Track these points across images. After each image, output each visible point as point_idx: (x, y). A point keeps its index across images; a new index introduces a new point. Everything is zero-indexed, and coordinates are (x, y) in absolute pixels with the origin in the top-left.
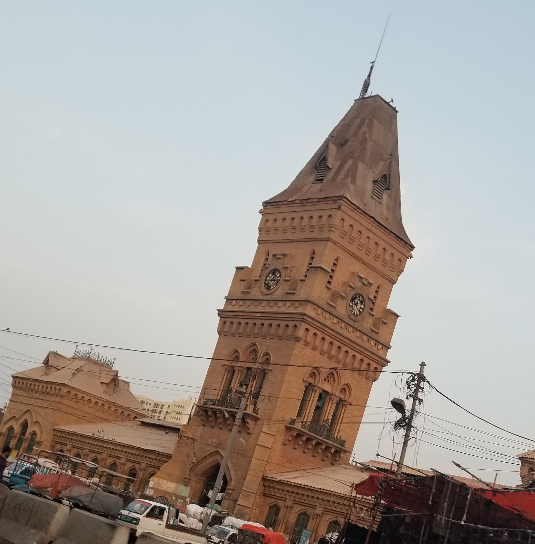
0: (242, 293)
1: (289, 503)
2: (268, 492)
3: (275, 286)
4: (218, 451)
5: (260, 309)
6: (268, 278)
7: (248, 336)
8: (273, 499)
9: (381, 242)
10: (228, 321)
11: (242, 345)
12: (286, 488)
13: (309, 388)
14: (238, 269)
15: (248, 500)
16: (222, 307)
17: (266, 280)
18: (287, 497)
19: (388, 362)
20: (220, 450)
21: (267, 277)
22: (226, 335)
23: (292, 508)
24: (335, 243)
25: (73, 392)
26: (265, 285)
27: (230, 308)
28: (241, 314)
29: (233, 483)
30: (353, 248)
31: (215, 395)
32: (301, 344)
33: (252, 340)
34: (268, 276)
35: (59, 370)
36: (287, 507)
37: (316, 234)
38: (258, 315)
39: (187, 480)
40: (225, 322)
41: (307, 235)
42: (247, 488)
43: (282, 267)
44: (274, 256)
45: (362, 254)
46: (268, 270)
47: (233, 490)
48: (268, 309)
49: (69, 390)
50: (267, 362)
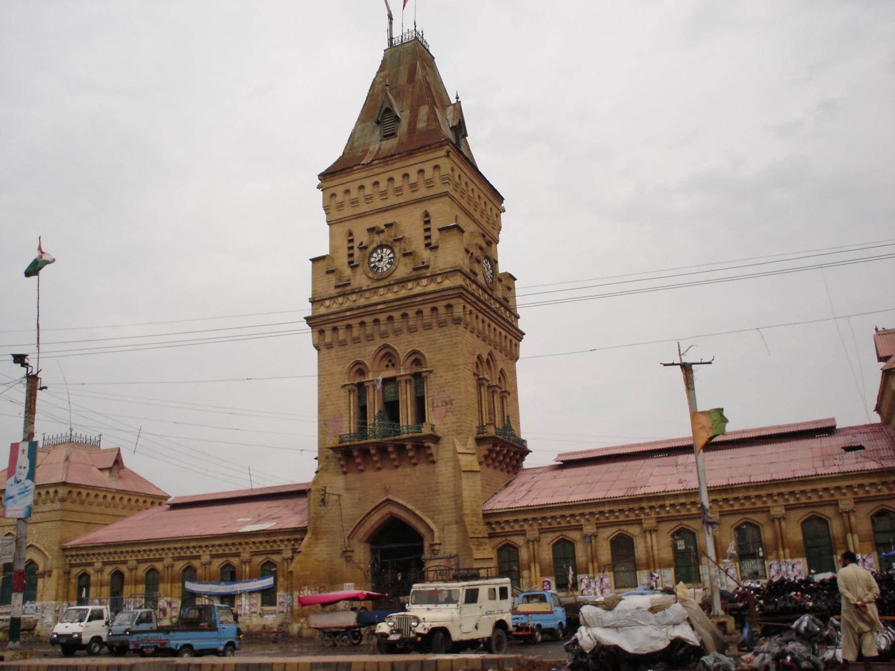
0: (337, 287)
1: (533, 533)
3: (389, 266)
4: (388, 500)
5: (376, 299)
6: (373, 260)
7: (370, 338)
9: (482, 196)
11: (368, 353)
13: (480, 382)
14: (314, 260)
16: (309, 313)
18: (526, 527)
19: (523, 334)
20: (390, 497)
21: (369, 259)
22: (329, 346)
24: (452, 198)
25: (76, 490)
27: (322, 310)
28: (348, 313)
29: (436, 534)
30: (464, 203)
31: (347, 426)
33: (379, 342)
36: (533, 541)
37: (423, 192)
38: (380, 307)
41: (408, 196)
42: (474, 533)
43: (391, 240)
44: (371, 230)
45: (471, 210)
48: (391, 296)
50: (418, 362)
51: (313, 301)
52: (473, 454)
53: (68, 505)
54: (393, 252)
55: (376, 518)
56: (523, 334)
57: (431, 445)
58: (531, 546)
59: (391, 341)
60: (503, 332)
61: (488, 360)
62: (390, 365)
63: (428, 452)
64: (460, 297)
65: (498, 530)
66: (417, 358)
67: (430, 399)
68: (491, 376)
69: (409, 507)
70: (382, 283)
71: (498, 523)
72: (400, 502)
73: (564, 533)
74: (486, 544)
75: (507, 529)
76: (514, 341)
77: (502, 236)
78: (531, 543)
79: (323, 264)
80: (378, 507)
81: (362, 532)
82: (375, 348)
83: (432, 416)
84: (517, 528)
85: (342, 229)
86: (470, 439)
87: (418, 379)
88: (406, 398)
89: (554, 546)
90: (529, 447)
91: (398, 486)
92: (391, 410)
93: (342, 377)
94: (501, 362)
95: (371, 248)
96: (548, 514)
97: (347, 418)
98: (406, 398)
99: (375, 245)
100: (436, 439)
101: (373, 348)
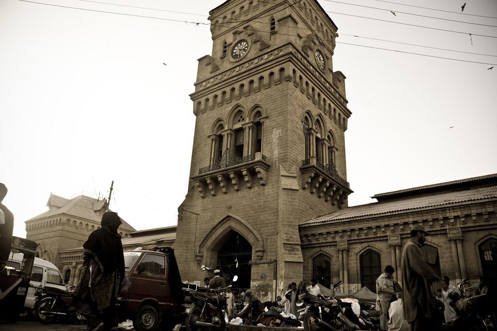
2: (306, 243)
4: (229, 216)
6: (234, 51)
8: (315, 249)
10: (203, 100)
12: (332, 229)
15: (295, 254)
17: (232, 53)
18: (338, 239)
19: (351, 113)
20: (230, 214)
23: (348, 251)
26: (233, 57)
27: (201, 88)
31: (206, 163)
32: (291, 84)
33: (234, 103)
34: (234, 49)
35: (60, 208)
36: (342, 251)
39: (198, 258)
40: (200, 103)
46: (233, 45)
47: (264, 251)
49: (68, 218)
51: (196, 85)
52: (296, 177)
53: (67, 228)
54: (247, 43)
55: (220, 231)
56: (351, 113)
57: (261, 170)
58: (340, 256)
59: (241, 101)
60: (332, 105)
61: (317, 120)
62: (241, 119)
63: (259, 176)
64: (290, 61)
65: (314, 242)
66: (257, 111)
67: (265, 138)
68: (321, 134)
69: (243, 221)
70: (238, 64)
71: (313, 235)
72: (237, 217)
73: (370, 244)
74: (298, 250)
75: (322, 240)
76: (343, 116)
77: (335, 51)
78: (340, 252)
79: (206, 61)
80: (222, 222)
81: (209, 243)
82: (230, 108)
83: (265, 150)
84: (330, 239)
85: (220, 41)
86: (294, 167)
87: (258, 126)
88: (247, 139)
89: (361, 256)
90: (351, 188)
91: (238, 206)
92: (239, 149)
93: (208, 130)
94: (330, 124)
95: (234, 43)
96: (357, 226)
97: (209, 159)
98: (247, 139)
99: (236, 41)
100: (267, 167)
101: (229, 108)
